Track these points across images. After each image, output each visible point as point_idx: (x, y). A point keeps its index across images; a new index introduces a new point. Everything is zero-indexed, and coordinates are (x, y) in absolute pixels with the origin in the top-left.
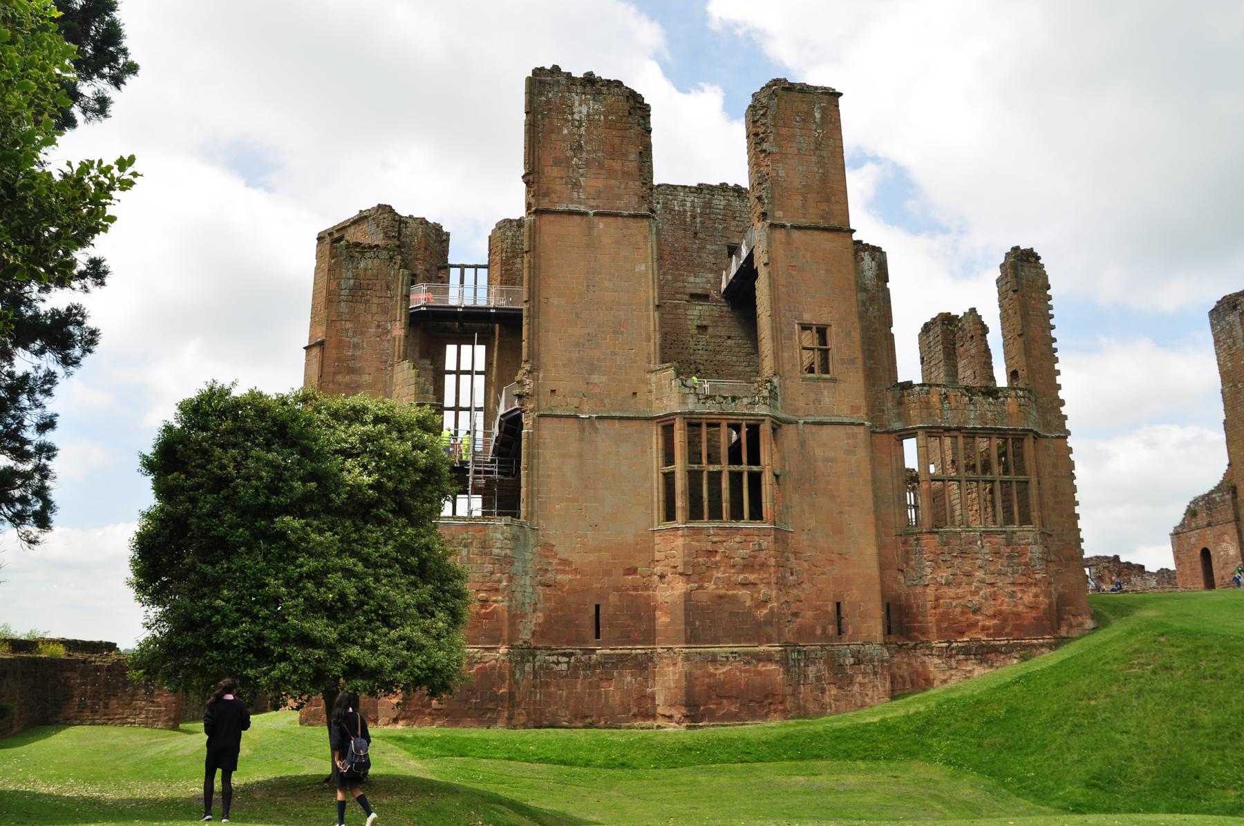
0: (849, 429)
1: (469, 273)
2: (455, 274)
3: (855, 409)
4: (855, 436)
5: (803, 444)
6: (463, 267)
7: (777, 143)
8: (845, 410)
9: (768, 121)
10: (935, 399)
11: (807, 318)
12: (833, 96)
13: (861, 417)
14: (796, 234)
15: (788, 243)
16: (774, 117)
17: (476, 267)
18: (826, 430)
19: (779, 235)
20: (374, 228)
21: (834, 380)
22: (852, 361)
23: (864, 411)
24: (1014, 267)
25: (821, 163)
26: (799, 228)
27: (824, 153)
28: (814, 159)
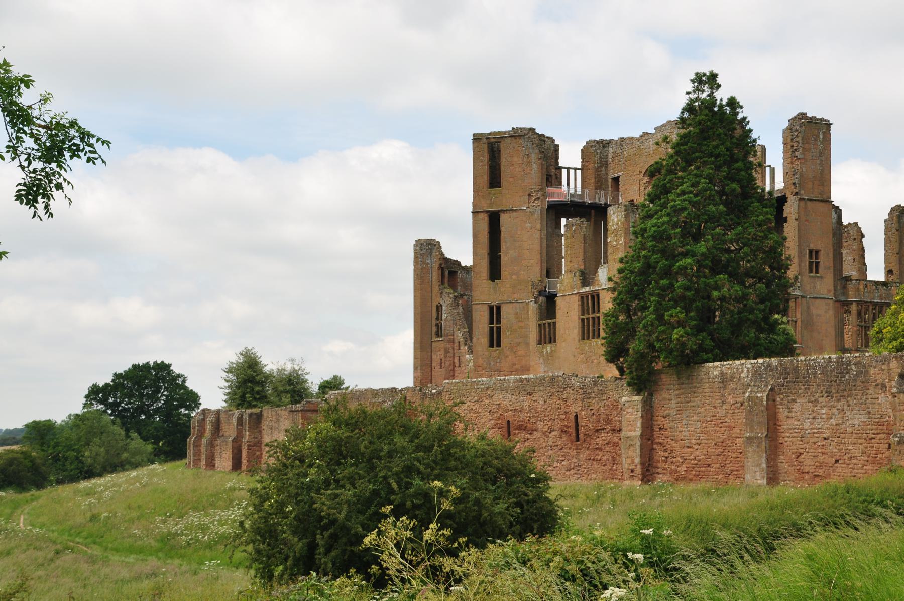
0: (827, 301)
1: (572, 172)
2: (564, 172)
3: (829, 291)
4: (828, 304)
5: (808, 308)
6: (568, 169)
7: (803, 153)
8: (825, 292)
9: (799, 139)
10: (861, 287)
11: (812, 246)
12: (828, 125)
13: (831, 296)
14: (809, 203)
15: (806, 208)
16: (803, 139)
17: (575, 169)
18: (818, 301)
19: (802, 203)
20: (530, 145)
21: (821, 277)
22: (829, 268)
23: (832, 293)
24: (899, 217)
25: (821, 164)
26: (811, 200)
27: (823, 158)
28: (818, 162)
